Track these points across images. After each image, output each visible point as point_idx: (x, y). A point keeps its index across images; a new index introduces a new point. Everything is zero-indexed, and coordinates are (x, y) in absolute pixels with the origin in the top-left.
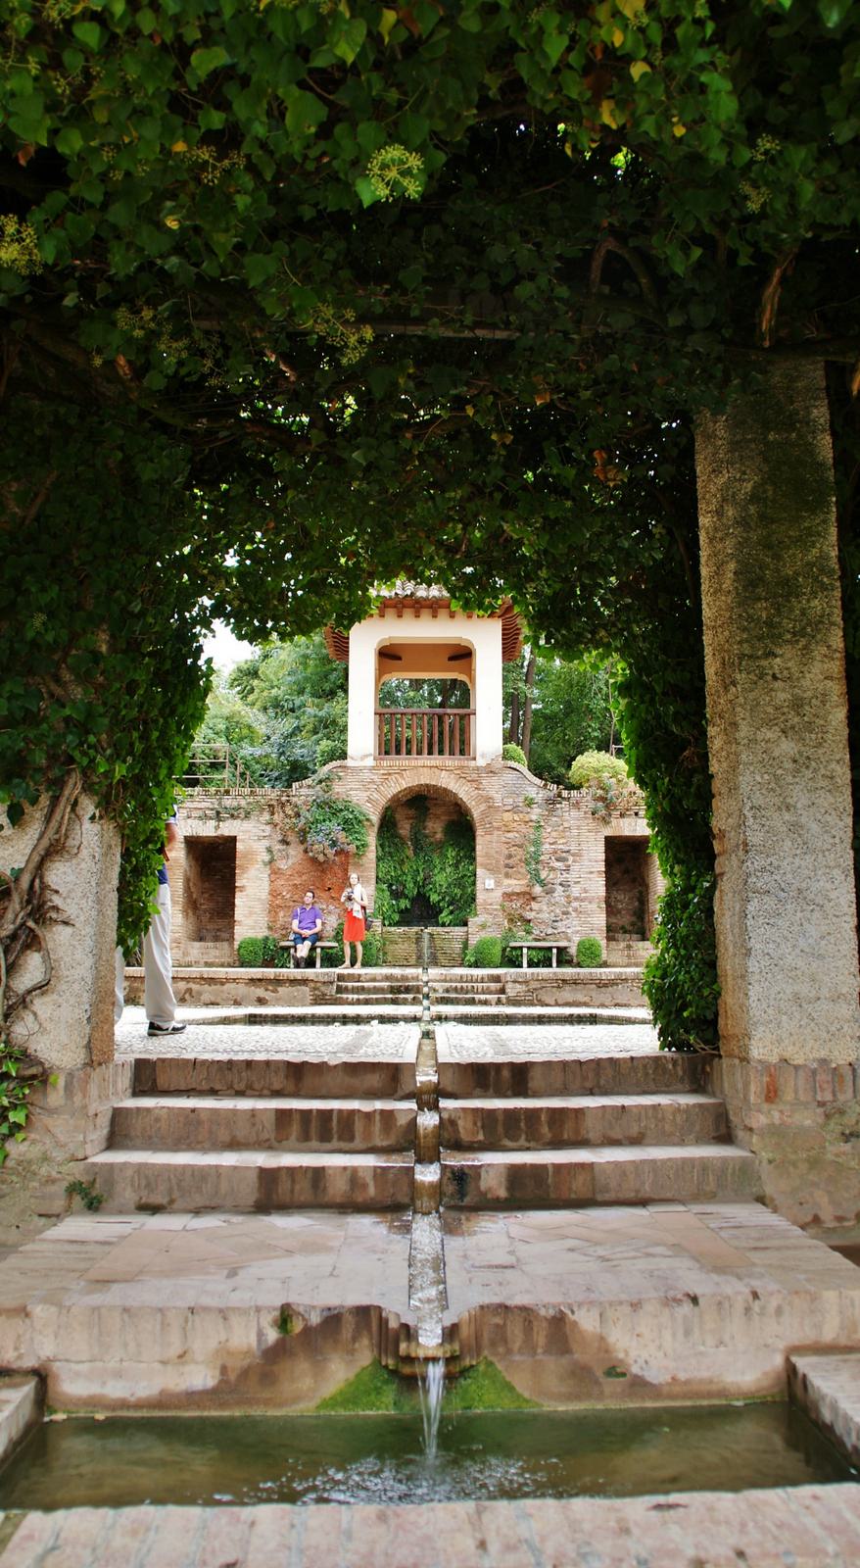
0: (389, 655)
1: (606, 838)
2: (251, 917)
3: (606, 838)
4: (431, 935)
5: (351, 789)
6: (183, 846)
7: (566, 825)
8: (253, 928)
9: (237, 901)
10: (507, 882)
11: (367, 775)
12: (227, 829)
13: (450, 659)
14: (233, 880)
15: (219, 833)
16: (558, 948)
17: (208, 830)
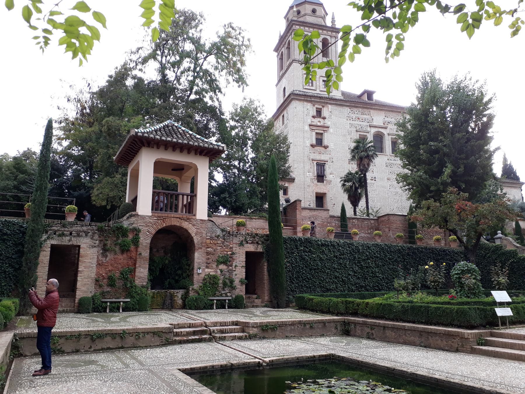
0: (159, 166)
1: (246, 252)
2: (85, 287)
3: (246, 252)
4: (170, 293)
5: (140, 226)
6: (49, 249)
7: (231, 246)
8: (85, 292)
9: (79, 278)
10: (206, 270)
11: (148, 219)
12: (75, 241)
13: (172, 170)
14: (78, 268)
15: (70, 243)
16: (228, 300)
17: (65, 241)
